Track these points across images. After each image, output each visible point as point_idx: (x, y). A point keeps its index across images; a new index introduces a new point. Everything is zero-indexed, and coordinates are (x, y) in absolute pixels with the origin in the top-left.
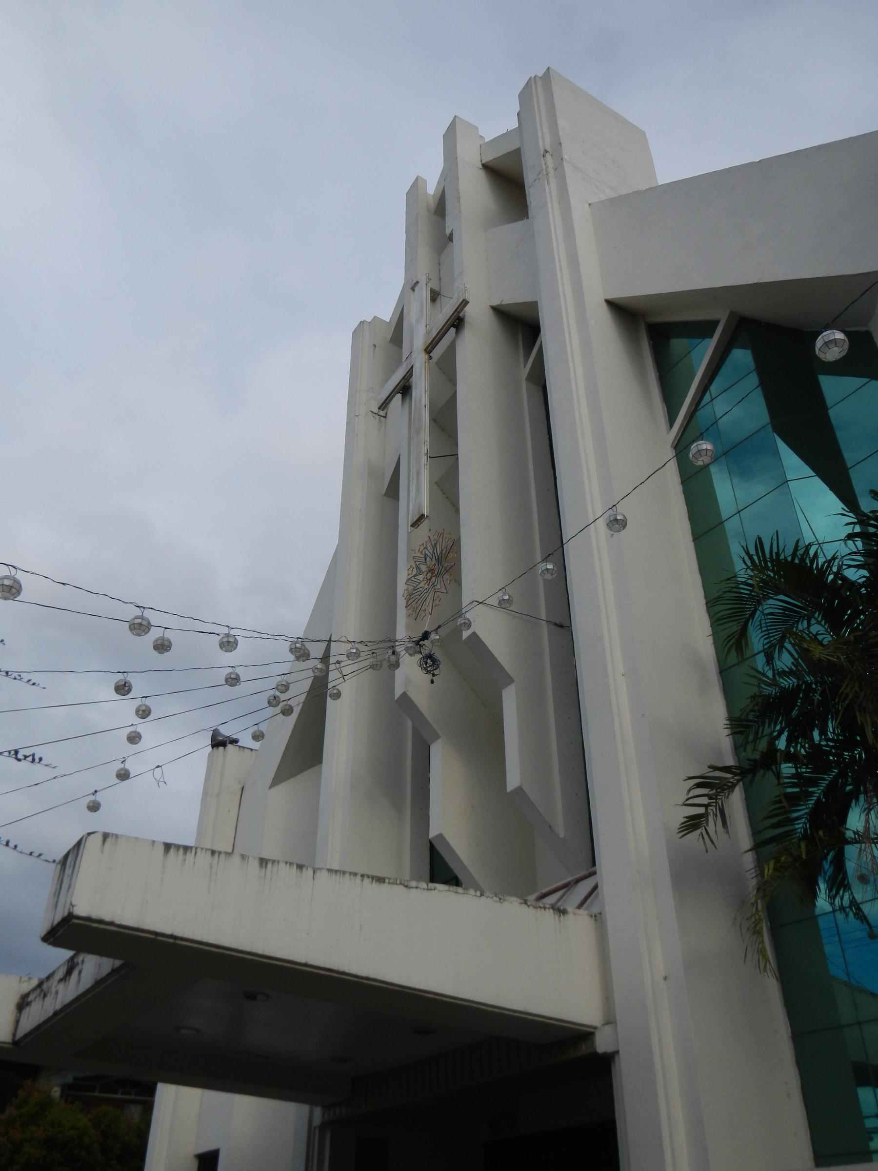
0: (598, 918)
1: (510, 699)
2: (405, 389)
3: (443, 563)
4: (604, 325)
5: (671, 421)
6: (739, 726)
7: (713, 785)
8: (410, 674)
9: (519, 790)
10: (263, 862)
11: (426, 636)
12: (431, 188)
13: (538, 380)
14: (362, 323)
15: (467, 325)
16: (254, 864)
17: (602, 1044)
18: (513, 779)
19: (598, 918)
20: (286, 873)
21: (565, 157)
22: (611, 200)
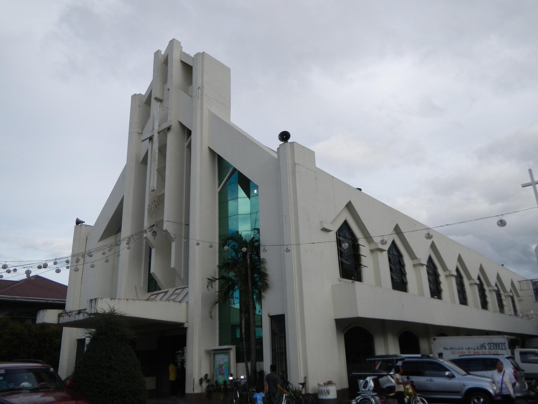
0: (187, 303)
1: (173, 245)
2: (151, 139)
3: (159, 202)
4: (206, 154)
5: (219, 186)
6: (220, 267)
7: (211, 281)
8: (148, 235)
9: (174, 268)
10: (127, 300)
11: (154, 225)
12: (163, 53)
13: (189, 146)
14: (135, 94)
15: (171, 130)
16: (125, 300)
17: (185, 326)
18: (173, 266)
19: (187, 303)
20: (131, 301)
21: (204, 93)
22: (214, 115)
